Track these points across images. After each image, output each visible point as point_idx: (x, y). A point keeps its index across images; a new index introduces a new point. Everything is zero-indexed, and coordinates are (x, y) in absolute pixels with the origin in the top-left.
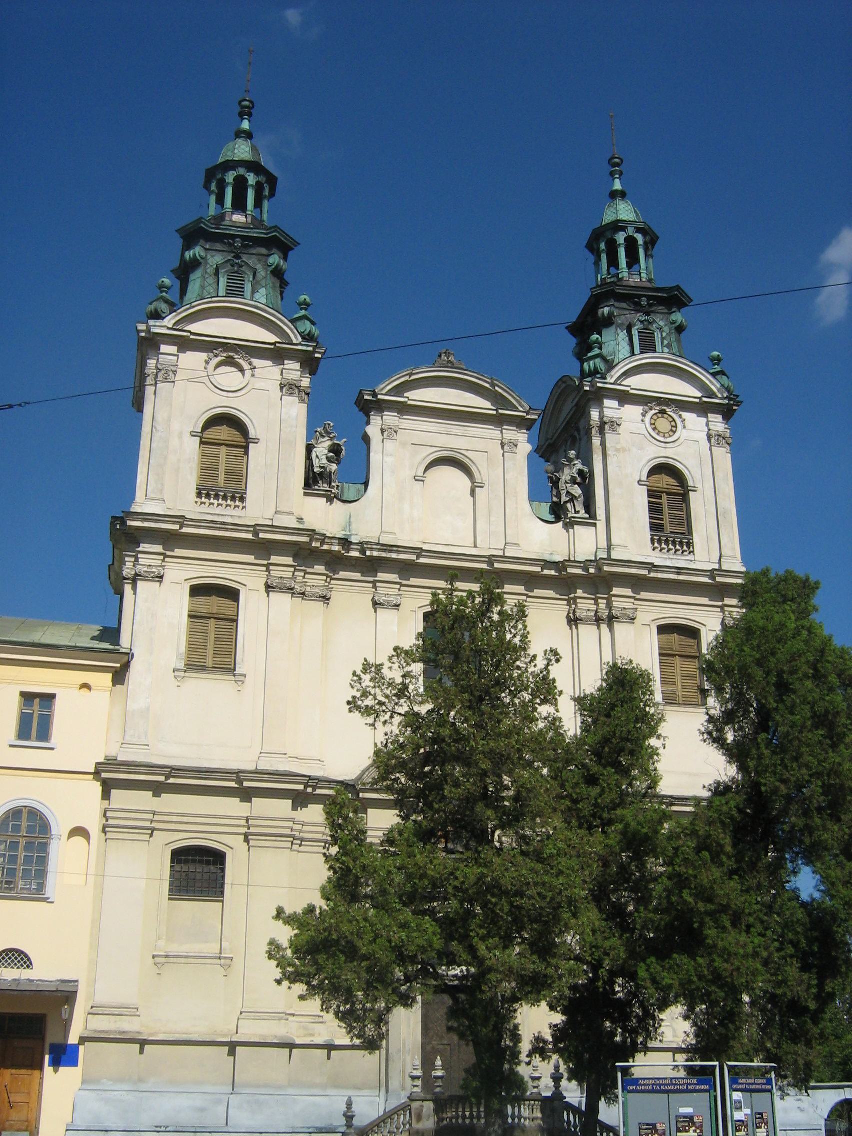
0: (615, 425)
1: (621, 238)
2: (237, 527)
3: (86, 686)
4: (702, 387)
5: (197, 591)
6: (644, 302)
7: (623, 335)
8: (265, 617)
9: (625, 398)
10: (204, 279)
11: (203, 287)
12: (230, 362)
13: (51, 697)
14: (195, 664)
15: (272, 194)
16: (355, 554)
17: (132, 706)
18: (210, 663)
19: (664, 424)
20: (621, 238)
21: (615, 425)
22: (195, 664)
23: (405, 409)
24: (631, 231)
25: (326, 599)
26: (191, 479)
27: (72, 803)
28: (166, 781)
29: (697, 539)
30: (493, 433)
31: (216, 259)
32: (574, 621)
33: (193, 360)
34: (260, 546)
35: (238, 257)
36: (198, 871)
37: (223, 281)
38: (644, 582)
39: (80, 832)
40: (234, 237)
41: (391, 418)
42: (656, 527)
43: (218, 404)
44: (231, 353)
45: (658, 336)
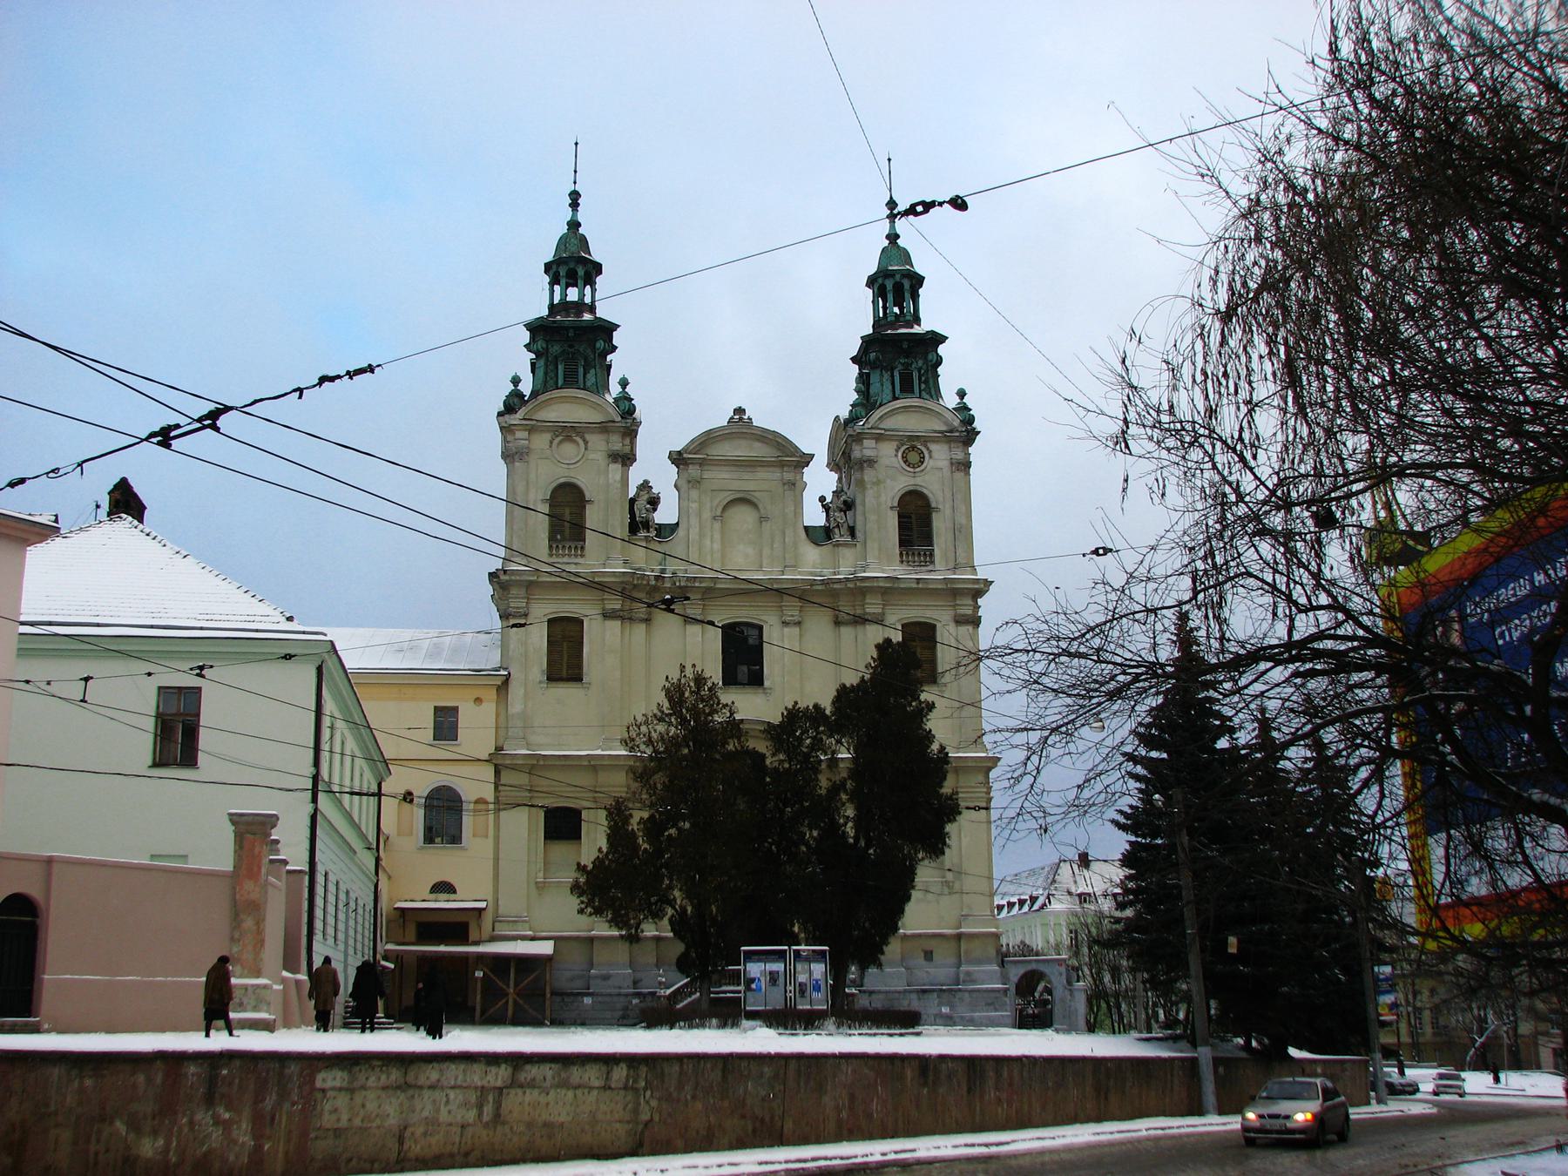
0: (871, 462)
1: (889, 285)
2: (576, 575)
3: (478, 700)
4: (946, 423)
5: (549, 621)
6: (905, 346)
7: (886, 376)
8: (602, 640)
9: (879, 438)
10: (546, 366)
11: (546, 374)
12: (569, 439)
13: (456, 709)
14: (553, 676)
15: (599, 272)
16: (668, 585)
17: (511, 710)
18: (564, 674)
19: (913, 457)
20: (889, 285)
21: (871, 462)
22: (553, 676)
23: (702, 463)
24: (898, 277)
25: (647, 621)
26: (544, 536)
27: (475, 785)
28: (536, 765)
29: (937, 552)
30: (775, 474)
31: (556, 349)
32: (838, 623)
33: (541, 441)
34: (596, 586)
35: (571, 346)
36: (562, 825)
37: (561, 367)
38: (891, 590)
39: (479, 801)
40: (567, 329)
41: (693, 471)
42: (904, 542)
43: (561, 475)
44: (568, 432)
45: (915, 375)
